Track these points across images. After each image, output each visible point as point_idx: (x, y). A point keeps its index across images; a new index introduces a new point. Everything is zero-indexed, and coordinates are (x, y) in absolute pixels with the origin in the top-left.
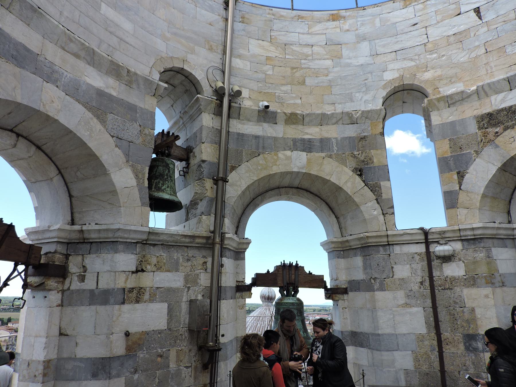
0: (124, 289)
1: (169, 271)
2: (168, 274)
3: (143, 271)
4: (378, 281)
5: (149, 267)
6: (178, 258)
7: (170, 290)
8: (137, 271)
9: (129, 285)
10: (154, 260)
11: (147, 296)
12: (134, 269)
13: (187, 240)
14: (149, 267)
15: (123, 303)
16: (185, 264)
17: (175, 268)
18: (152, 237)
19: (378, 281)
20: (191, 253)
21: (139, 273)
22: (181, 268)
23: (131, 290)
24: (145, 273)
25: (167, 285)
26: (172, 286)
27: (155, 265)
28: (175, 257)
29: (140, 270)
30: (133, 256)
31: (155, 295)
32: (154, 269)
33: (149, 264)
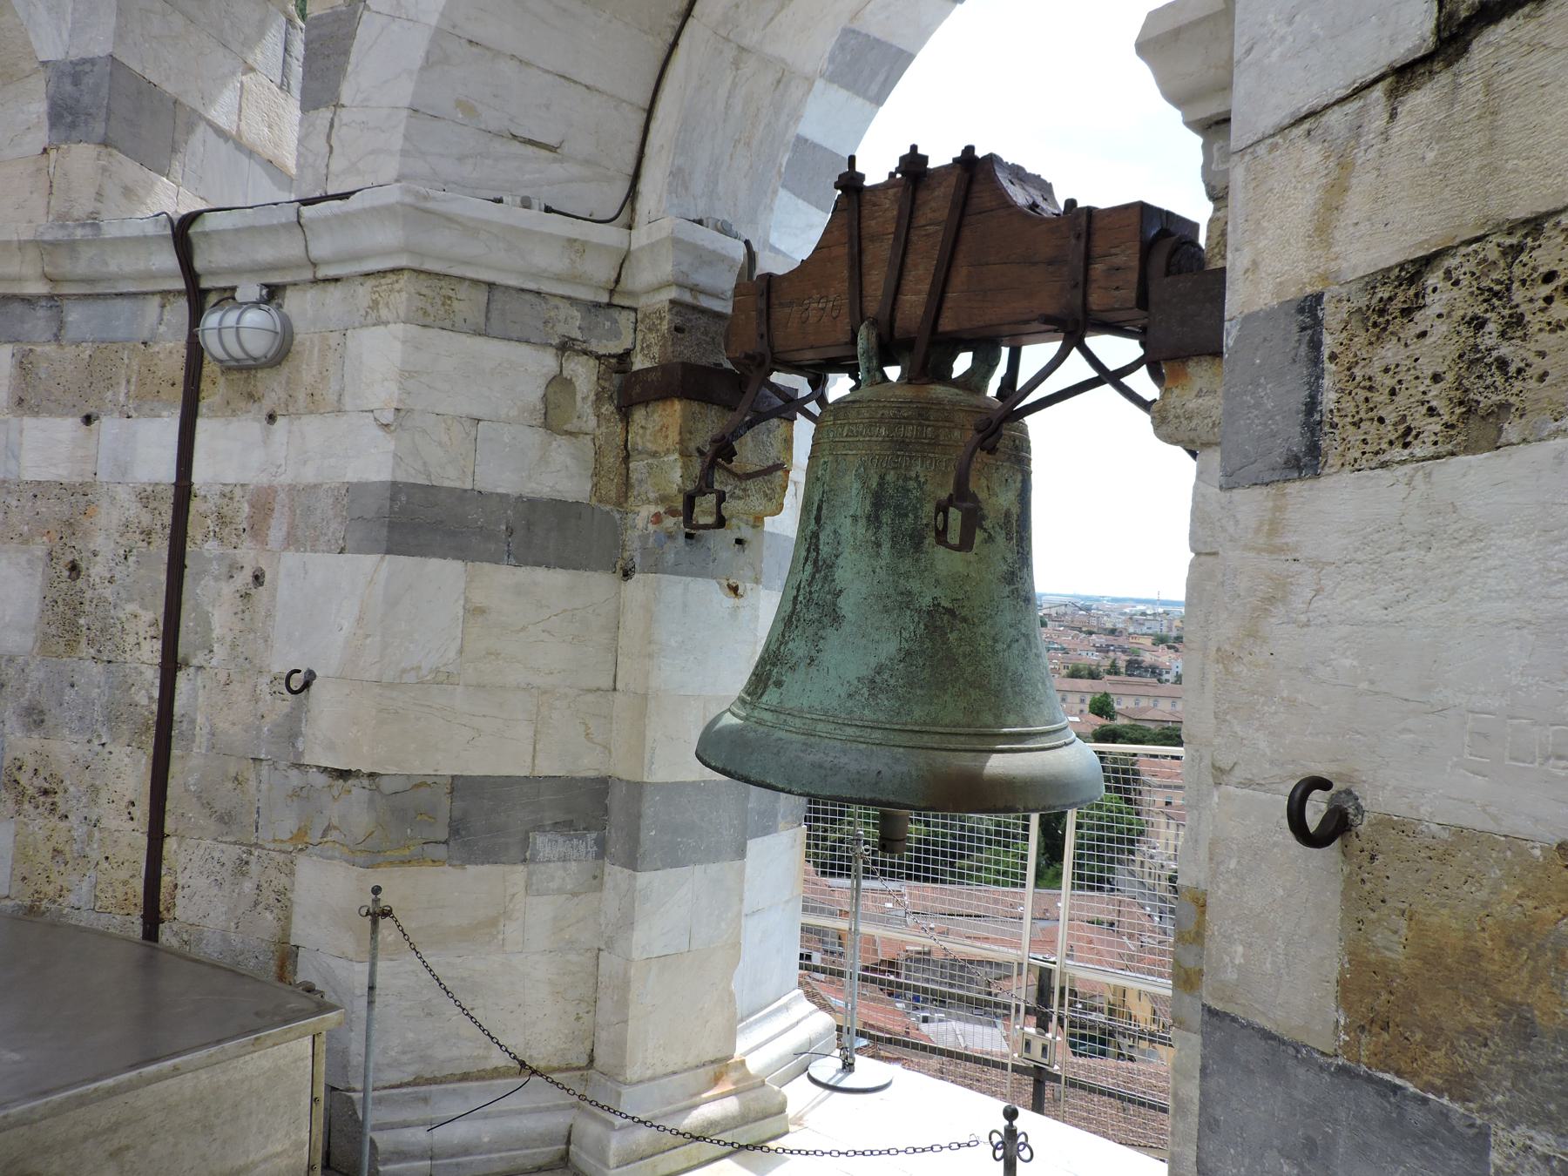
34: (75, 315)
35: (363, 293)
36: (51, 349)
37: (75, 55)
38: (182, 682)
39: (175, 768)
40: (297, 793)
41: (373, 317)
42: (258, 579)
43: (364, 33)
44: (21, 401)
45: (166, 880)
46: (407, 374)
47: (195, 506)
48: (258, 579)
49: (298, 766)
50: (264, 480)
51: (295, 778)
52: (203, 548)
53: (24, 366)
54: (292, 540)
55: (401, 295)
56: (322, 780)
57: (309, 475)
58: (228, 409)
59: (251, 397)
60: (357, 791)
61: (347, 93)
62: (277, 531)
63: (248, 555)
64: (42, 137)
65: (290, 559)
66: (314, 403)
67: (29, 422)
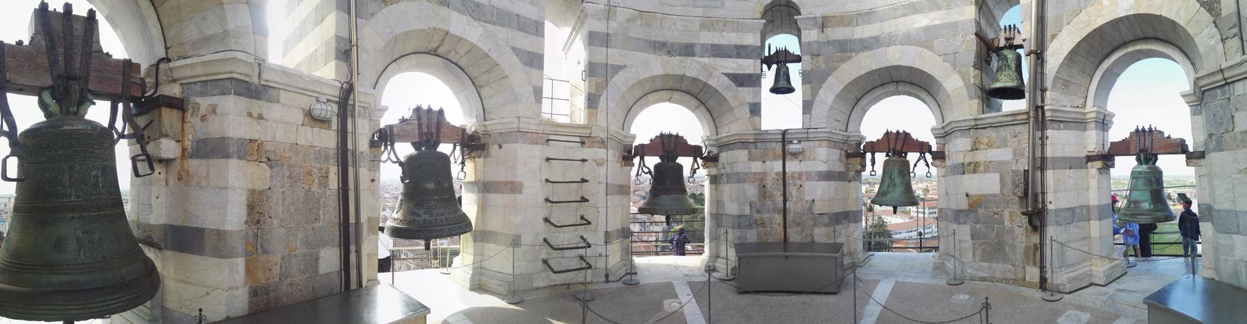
0: (963, 164)
1: (999, 148)
2: (999, 150)
3: (977, 149)
4: (1214, 138)
5: (981, 146)
6: (1006, 136)
7: (1001, 163)
8: (972, 150)
9: (967, 161)
10: (986, 140)
11: (982, 168)
12: (970, 149)
13: (1009, 119)
14: (981, 146)
15: (964, 173)
16: (1012, 140)
17: (1004, 144)
18: (979, 122)
19: (1214, 138)
20: (1018, 128)
21: (974, 152)
22: (1009, 144)
23: (970, 164)
24: (979, 151)
25: (998, 158)
26: (1003, 159)
27: (987, 144)
28: (1004, 136)
29: (974, 149)
30: (968, 139)
31: (989, 167)
32: (987, 147)
33: (982, 144)
34: (759, 145)
35: (818, 143)
36: (755, 150)
37: (754, 101)
38: (787, 203)
39: (787, 217)
40: (813, 218)
41: (820, 146)
42: (801, 186)
43: (815, 104)
44: (750, 159)
45: (788, 235)
46: (828, 155)
47: (787, 175)
48: (801, 186)
49: (813, 214)
50: (800, 171)
51: (812, 216)
52: (789, 181)
53: (750, 153)
54: (807, 180)
55: (826, 143)
56: (817, 216)
57: (809, 170)
58: (792, 160)
59: (796, 158)
60: (825, 216)
61: (813, 112)
62: (804, 178)
63: (798, 182)
64: (749, 115)
65: (807, 183)
66: (809, 159)
67: (752, 162)
